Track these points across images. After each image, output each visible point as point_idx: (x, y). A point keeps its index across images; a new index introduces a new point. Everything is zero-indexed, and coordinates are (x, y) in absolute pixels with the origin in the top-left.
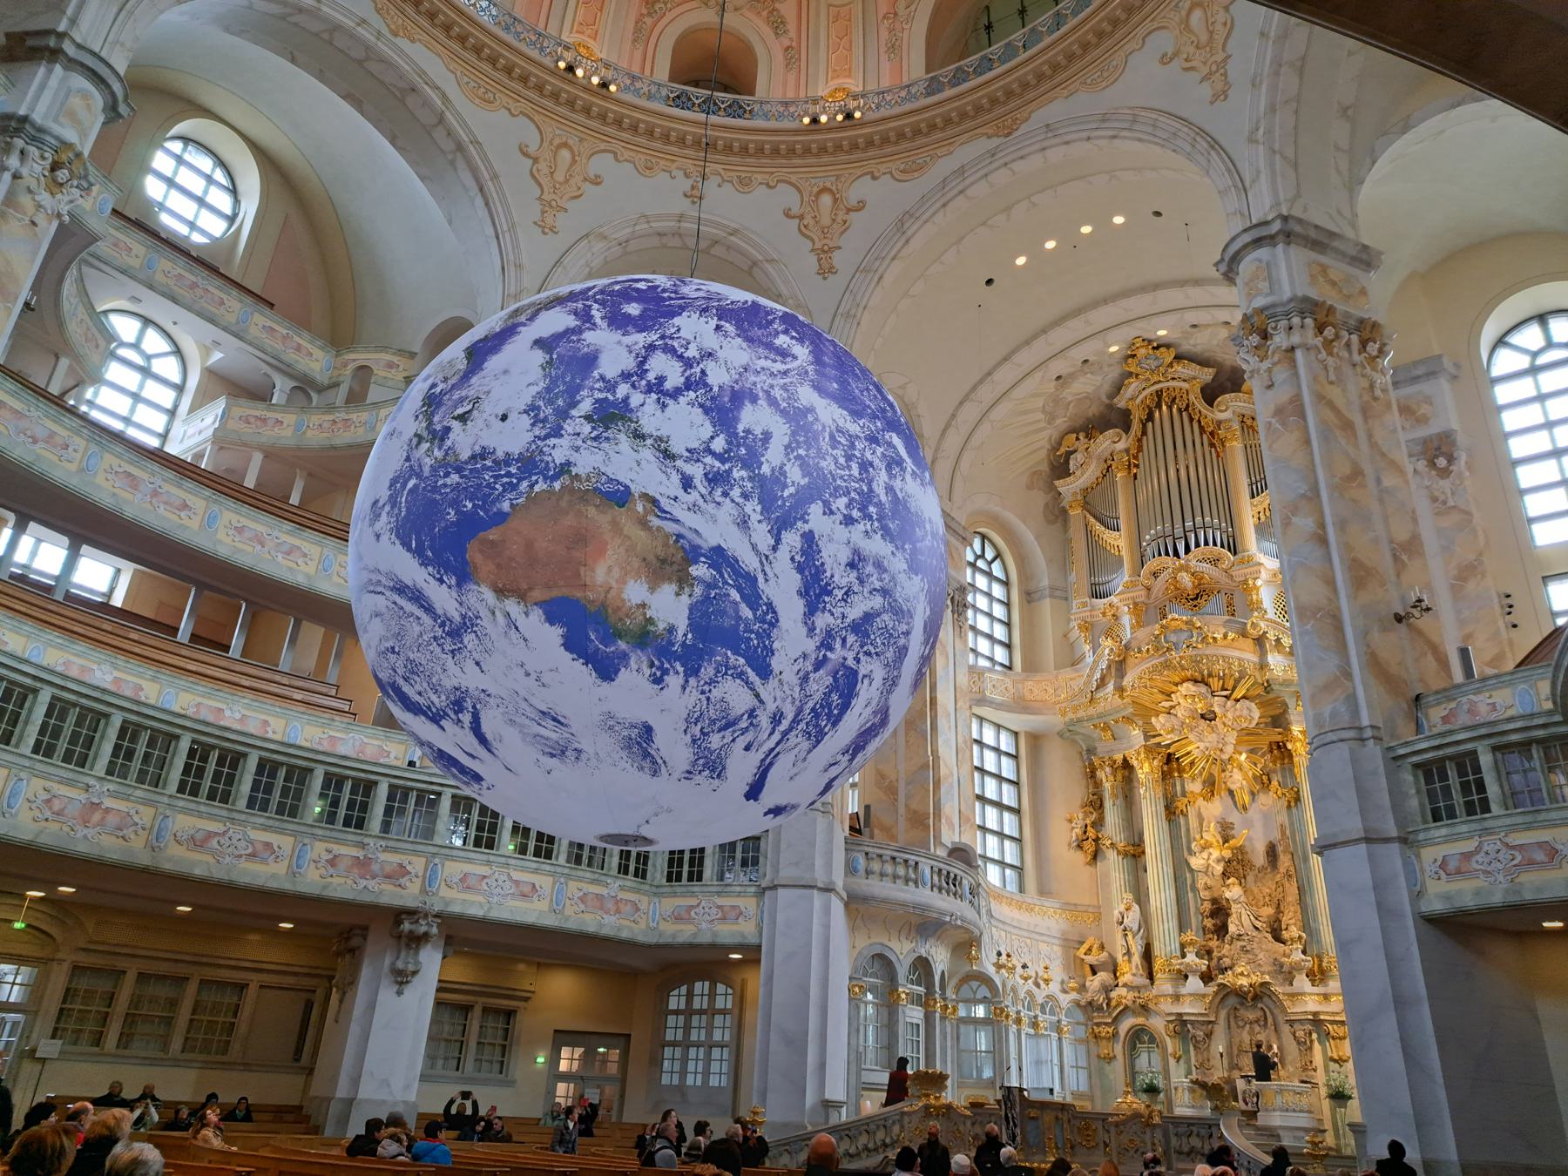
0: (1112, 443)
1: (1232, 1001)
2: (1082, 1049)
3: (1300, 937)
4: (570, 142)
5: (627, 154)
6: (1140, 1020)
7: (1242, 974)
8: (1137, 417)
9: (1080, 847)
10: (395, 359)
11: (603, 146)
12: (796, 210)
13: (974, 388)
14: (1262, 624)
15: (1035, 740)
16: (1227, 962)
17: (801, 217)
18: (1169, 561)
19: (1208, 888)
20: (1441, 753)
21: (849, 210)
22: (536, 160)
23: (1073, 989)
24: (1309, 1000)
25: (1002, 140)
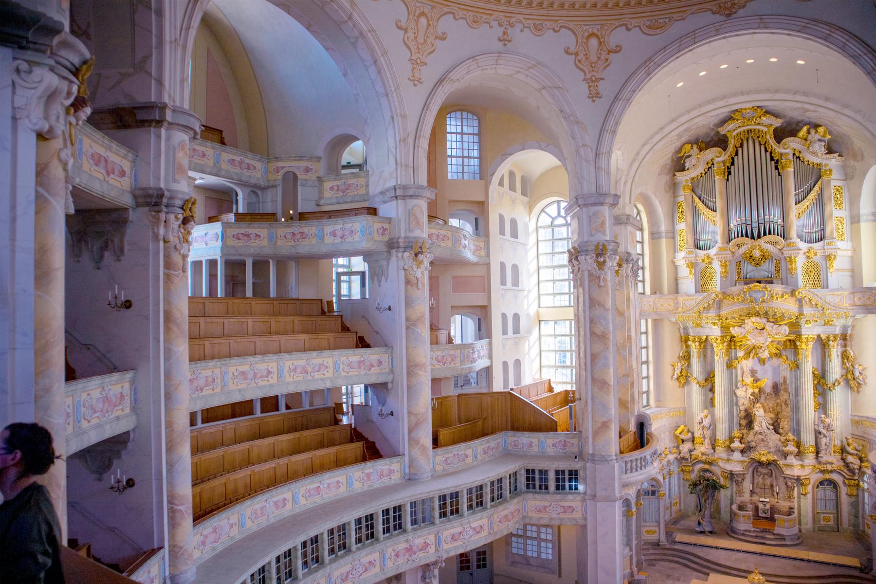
0: (712, 153)
4: (426, 11)
5: (461, 13)
8: (732, 143)
10: (309, 164)
11: (446, 10)
12: (573, 49)
13: (652, 137)
16: (753, 444)
17: (577, 54)
18: (749, 240)
19: (743, 404)
21: (610, 52)
22: (406, 30)
25: (723, 18)
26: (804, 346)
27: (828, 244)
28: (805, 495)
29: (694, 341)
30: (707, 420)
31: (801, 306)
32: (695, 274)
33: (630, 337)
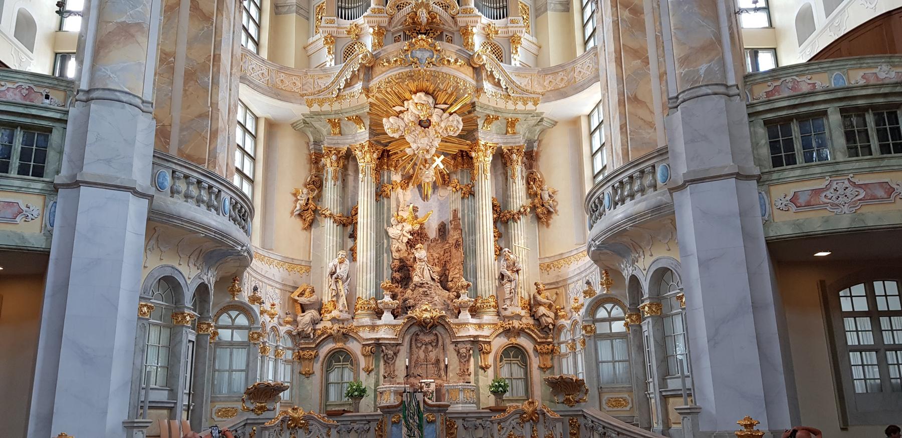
1: (415, 329)
2: (289, 367)
3: (468, 285)
6: (340, 345)
7: (426, 310)
9: (300, 215)
14: (484, 57)
15: (272, 125)
16: (411, 302)
19: (398, 251)
20: (796, 111)
23: (288, 323)
24: (469, 327)
26: (482, 159)
27: (512, 22)
28: (485, 368)
29: (328, 155)
30: (343, 266)
31: (479, 79)
32: (335, 53)
33: (217, 58)
